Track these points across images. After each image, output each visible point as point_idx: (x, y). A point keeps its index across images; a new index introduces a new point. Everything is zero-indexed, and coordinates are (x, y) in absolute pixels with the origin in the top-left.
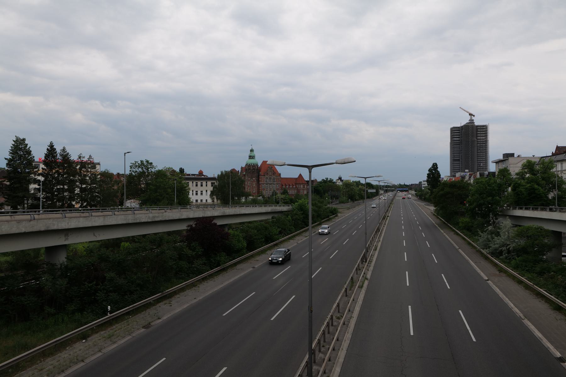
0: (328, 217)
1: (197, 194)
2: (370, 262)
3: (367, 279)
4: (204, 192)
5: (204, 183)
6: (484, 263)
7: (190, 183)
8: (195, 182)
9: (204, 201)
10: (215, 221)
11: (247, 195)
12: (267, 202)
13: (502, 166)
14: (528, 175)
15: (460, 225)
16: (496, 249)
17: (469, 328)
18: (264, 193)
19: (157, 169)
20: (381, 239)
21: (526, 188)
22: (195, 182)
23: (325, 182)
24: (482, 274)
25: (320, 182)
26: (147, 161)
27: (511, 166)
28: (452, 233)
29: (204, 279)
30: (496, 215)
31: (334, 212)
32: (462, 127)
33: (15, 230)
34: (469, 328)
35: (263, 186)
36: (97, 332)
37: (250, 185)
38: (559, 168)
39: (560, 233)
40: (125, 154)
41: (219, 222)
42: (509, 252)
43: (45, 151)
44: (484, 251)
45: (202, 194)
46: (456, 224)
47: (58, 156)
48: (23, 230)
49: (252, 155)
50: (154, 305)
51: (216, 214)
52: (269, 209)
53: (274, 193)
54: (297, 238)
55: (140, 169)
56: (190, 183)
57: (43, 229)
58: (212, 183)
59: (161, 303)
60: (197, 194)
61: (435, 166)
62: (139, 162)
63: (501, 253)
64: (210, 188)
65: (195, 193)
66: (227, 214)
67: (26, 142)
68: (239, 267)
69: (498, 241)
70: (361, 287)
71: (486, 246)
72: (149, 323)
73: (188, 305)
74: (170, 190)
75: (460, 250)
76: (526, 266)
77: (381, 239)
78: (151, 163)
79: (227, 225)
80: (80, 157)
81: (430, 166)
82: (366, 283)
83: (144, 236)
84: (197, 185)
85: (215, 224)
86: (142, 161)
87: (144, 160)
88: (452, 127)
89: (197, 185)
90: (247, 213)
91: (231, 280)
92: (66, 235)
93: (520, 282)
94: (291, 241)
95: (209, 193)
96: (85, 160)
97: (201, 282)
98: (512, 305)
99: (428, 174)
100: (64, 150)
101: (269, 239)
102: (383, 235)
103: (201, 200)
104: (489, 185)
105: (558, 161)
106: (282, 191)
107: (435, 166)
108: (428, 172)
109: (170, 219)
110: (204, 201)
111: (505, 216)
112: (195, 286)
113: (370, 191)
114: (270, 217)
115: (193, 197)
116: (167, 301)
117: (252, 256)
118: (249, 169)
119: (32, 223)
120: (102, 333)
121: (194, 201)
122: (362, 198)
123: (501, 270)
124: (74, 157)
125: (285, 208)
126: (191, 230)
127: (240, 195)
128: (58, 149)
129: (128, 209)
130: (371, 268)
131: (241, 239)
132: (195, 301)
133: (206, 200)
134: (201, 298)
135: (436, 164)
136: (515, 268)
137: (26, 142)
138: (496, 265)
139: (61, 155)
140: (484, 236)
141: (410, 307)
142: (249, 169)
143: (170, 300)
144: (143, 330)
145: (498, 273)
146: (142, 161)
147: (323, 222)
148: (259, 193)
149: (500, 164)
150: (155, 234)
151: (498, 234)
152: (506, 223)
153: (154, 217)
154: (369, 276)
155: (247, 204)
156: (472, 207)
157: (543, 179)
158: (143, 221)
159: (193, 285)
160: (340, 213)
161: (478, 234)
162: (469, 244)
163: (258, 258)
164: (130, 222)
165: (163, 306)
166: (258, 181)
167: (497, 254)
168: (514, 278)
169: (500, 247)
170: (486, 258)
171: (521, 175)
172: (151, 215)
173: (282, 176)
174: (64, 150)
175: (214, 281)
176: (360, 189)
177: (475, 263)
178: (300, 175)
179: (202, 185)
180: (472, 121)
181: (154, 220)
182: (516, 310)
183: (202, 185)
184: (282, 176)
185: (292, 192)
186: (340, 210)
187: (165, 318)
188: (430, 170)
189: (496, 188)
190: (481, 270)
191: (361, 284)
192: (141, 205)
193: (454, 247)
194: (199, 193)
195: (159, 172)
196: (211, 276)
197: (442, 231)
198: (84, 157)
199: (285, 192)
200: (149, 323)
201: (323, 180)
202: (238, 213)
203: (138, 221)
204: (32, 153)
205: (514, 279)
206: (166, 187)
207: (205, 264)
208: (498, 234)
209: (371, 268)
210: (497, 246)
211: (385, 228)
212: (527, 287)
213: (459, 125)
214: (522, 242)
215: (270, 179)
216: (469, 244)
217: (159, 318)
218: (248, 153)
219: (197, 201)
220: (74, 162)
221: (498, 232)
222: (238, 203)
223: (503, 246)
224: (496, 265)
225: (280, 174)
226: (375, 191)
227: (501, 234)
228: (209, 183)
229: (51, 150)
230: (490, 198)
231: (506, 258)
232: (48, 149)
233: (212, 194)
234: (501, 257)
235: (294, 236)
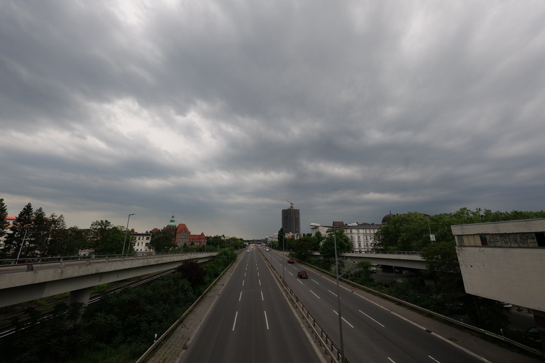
5: (141, 237)
16: (345, 275)
18: (178, 244)
23: (215, 237)
26: (106, 221)
29: (195, 306)
31: (236, 256)
33: (76, 274)
36: (149, 360)
38: (345, 232)
42: (351, 275)
43: (21, 210)
45: (138, 245)
47: (34, 215)
48: (82, 274)
49: (173, 219)
53: (185, 245)
54: (227, 273)
56: (138, 238)
57: (94, 272)
62: (100, 222)
67: (3, 202)
69: (345, 270)
72: (185, 344)
74: (122, 242)
80: (52, 216)
86: (101, 221)
87: (104, 220)
92: (101, 277)
93: (369, 292)
95: (144, 244)
96: (56, 218)
100: (40, 210)
101: (216, 275)
106: (190, 243)
115: (136, 247)
119: (89, 267)
120: (153, 359)
122: (241, 248)
123: (354, 286)
124: (48, 215)
125: (215, 254)
126: (179, 269)
127: (169, 246)
128: (35, 209)
132: (202, 323)
137: (3, 202)
138: (349, 283)
139: (36, 214)
140: (334, 268)
144: (184, 351)
146: (101, 221)
153: (158, 261)
157: (341, 237)
158: (152, 264)
159: (191, 311)
162: (324, 272)
167: (347, 277)
168: (364, 290)
174: (40, 210)
180: (292, 207)
185: (197, 244)
187: (192, 339)
195: (115, 229)
196: (198, 303)
198: (56, 216)
200: (185, 344)
203: (149, 264)
204: (7, 211)
213: (286, 209)
214: (357, 270)
217: (189, 340)
220: (46, 220)
228: (145, 238)
229: (28, 209)
232: (24, 209)
233: (147, 244)
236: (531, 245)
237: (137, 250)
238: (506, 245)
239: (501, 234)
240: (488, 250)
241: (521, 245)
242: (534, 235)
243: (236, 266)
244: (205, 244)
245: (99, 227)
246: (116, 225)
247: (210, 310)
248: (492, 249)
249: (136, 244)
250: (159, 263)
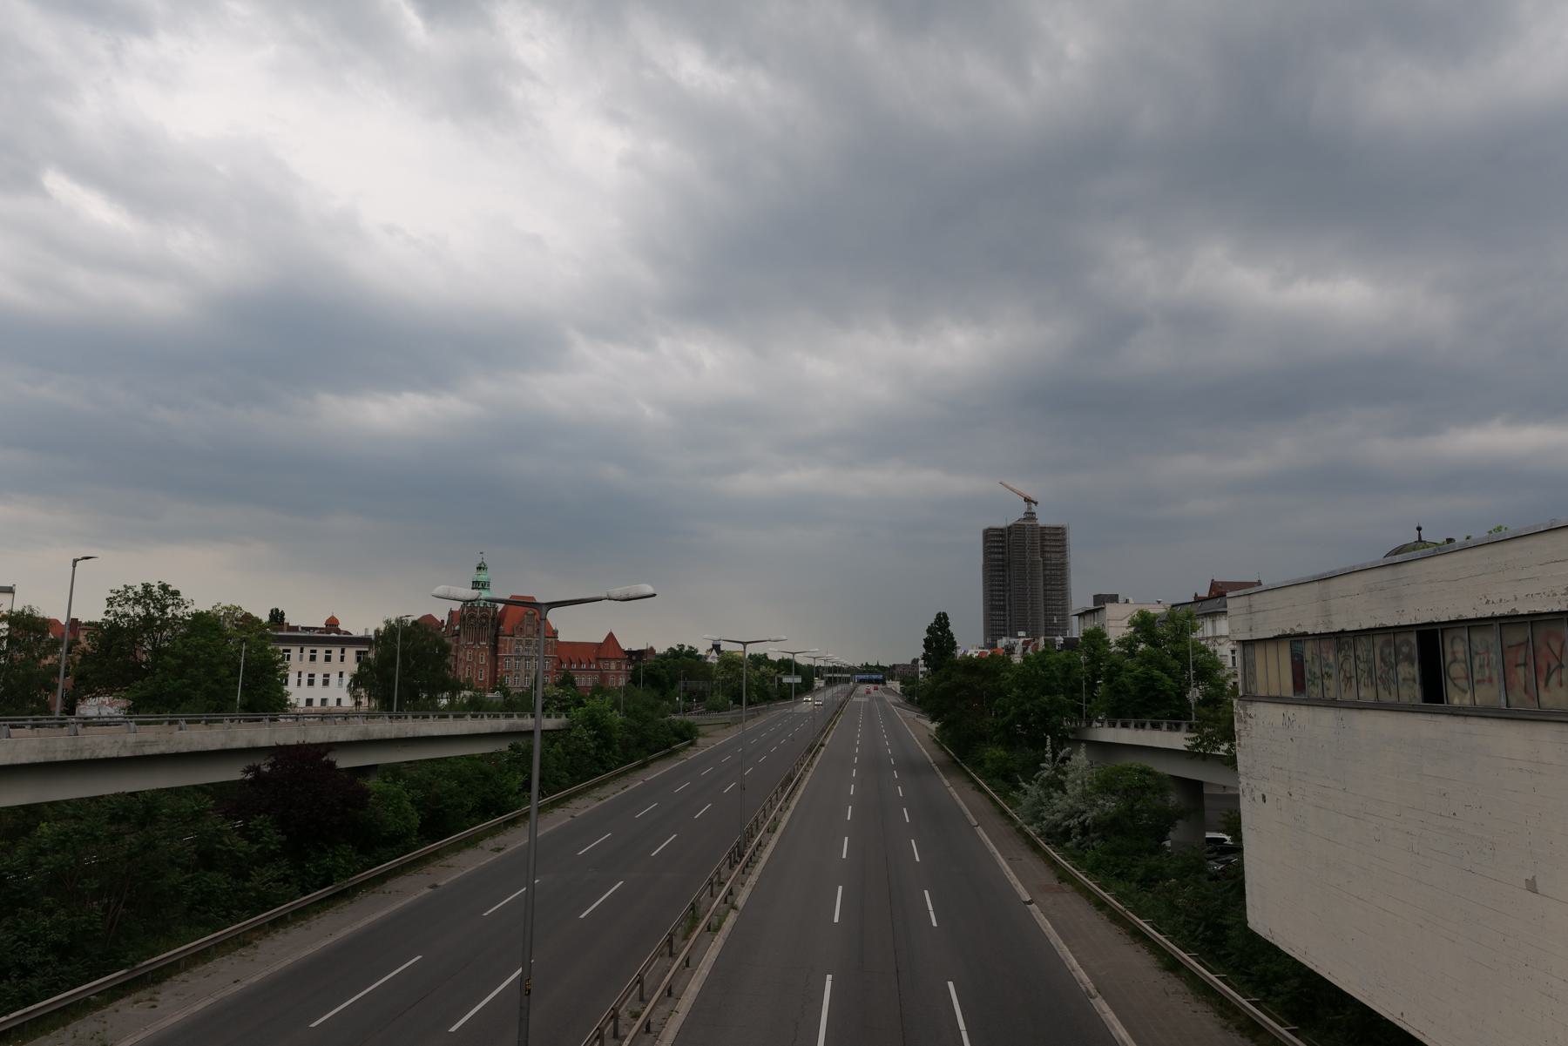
0: (669, 746)
1: (311, 683)
2: (752, 861)
3: (735, 908)
4: (334, 678)
6: (1029, 860)
7: (295, 651)
8: (307, 651)
9: (332, 703)
10: (331, 757)
11: (455, 688)
12: (514, 704)
13: (1090, 624)
14: (1142, 646)
15: (988, 765)
16: (1057, 826)
17: (962, 1026)
18: (509, 681)
19: (192, 609)
20: (793, 806)
21: (1136, 678)
22: (307, 651)
24: (1020, 888)
25: (664, 656)
26: (164, 587)
27: (1112, 623)
28: (969, 787)
29: (278, 923)
30: (1061, 741)
31: (687, 735)
34: (962, 1026)
35: (506, 665)
37: (470, 661)
39: (1198, 785)
40: (75, 561)
41: (344, 762)
42: (1085, 831)
44: (1029, 829)
45: (326, 683)
46: (978, 764)
49: (483, 577)
50: (98, 1007)
51: (342, 733)
52: (502, 724)
54: (576, 803)
55: (139, 610)
56: (295, 651)
58: (358, 653)
59: (123, 1001)
60: (311, 683)
61: (942, 621)
62: (139, 589)
63: (1067, 834)
64: (351, 665)
65: (305, 678)
66: (376, 736)
68: (391, 885)
70: (712, 929)
71: (1036, 817)
73: (211, 1001)
75: (980, 830)
76: (1117, 865)
77: (793, 806)
78: (176, 593)
79: (375, 766)
82: (732, 917)
83: (95, 799)
84: (313, 658)
85: (332, 764)
86: (146, 587)
89: (313, 658)
90: (436, 733)
91: (360, 925)
93: (1101, 905)
94: (557, 811)
95: (347, 679)
97: (266, 934)
98: (1074, 962)
101: (490, 807)
102: (800, 792)
103: (324, 701)
104: (1043, 668)
105: (1206, 615)
107: (942, 621)
108: (926, 635)
109: (193, 749)
110: (332, 703)
111: (1078, 742)
112: (244, 945)
113: (786, 680)
114: (504, 746)
115: (297, 693)
116: (143, 994)
117: (436, 855)
118: (472, 617)
121: (302, 704)
123: (1064, 877)
126: (259, 779)
129: (87, 722)
130: (753, 879)
131: (406, 804)
132: (238, 987)
133: (339, 701)
134: (255, 979)
136: (1093, 871)
141: (829, 977)
142: (472, 617)
143: (156, 988)
145: (1056, 883)
146: (146, 587)
147: (653, 761)
148: (496, 683)
149: (1088, 618)
150: (133, 794)
151: (1061, 786)
152: (1080, 758)
153: (141, 744)
154: (741, 901)
155: (457, 711)
156: (1006, 719)
157: (1175, 656)
160: (703, 735)
161: (1017, 788)
163: (453, 860)
164: (60, 757)
165: (126, 1008)
166: (495, 649)
167: (1058, 836)
169: (1064, 819)
170: (1035, 847)
171: (1128, 644)
172: (131, 738)
173: (561, 638)
175: (309, 929)
176: (763, 674)
177: (1009, 860)
178: (611, 636)
179: (328, 659)
180: (1030, 516)
181: (139, 753)
182: (1081, 975)
183: (328, 659)
184: (561, 638)
186: (701, 730)
189: (1057, 674)
190: (1016, 874)
191: (715, 921)
192: (134, 709)
193: (969, 823)
194: (319, 679)
195: (198, 616)
196: (301, 914)
197: (947, 783)
199: (567, 681)
201: (671, 649)
202: (410, 734)
203: (86, 755)
205: (1088, 898)
206: (216, 661)
207: (286, 879)
209: (753, 879)
210: (1059, 816)
212: (1116, 918)
213: (1001, 523)
214: (1110, 805)
215: (529, 643)
216: (1003, 812)
218: (474, 575)
219: (309, 702)
221: (1062, 783)
222: (426, 710)
223: (1072, 817)
224: (1053, 863)
225: (555, 633)
226: (798, 680)
227: (1068, 787)
228: (351, 653)
230: (1046, 698)
231: (1079, 845)
233: (357, 681)
234: (1068, 845)
235: (568, 798)
236: (1405, 699)
237: (309, 702)
238: (1350, 695)
239: (1340, 638)
240: (1302, 714)
241: (1384, 697)
242: (1413, 639)
243: (658, 771)
244: (622, 682)
245: (139, 610)
246: (203, 604)
247: (330, 940)
248: (1327, 717)
249: (293, 678)
250: (149, 751)
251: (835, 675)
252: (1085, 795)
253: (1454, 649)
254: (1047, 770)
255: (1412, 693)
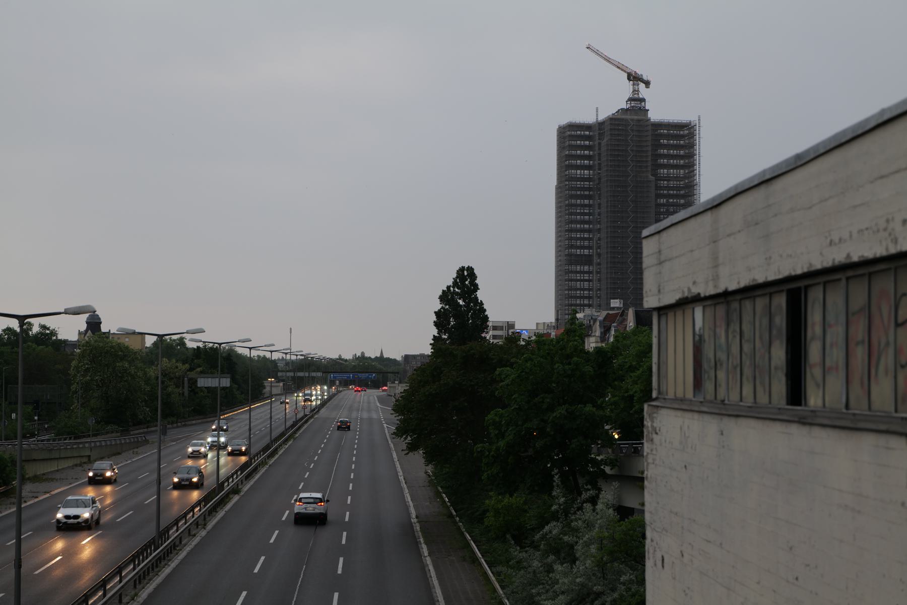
15: (490, 519)
20: (144, 595)
32: (601, 124)
61: (466, 280)
81: (447, 279)
88: (564, 121)
99: (438, 314)
107: (466, 280)
108: (438, 306)
135: (471, 270)
160: (36, 479)
176: (165, 374)
180: (637, 105)
188: (445, 297)
208: (568, 555)
211: (197, 540)
213: (588, 117)
226: (226, 382)
242: (781, 301)
251: (305, 371)
252: (601, 565)
253: (825, 316)
254: (553, 528)
255: (780, 387)
